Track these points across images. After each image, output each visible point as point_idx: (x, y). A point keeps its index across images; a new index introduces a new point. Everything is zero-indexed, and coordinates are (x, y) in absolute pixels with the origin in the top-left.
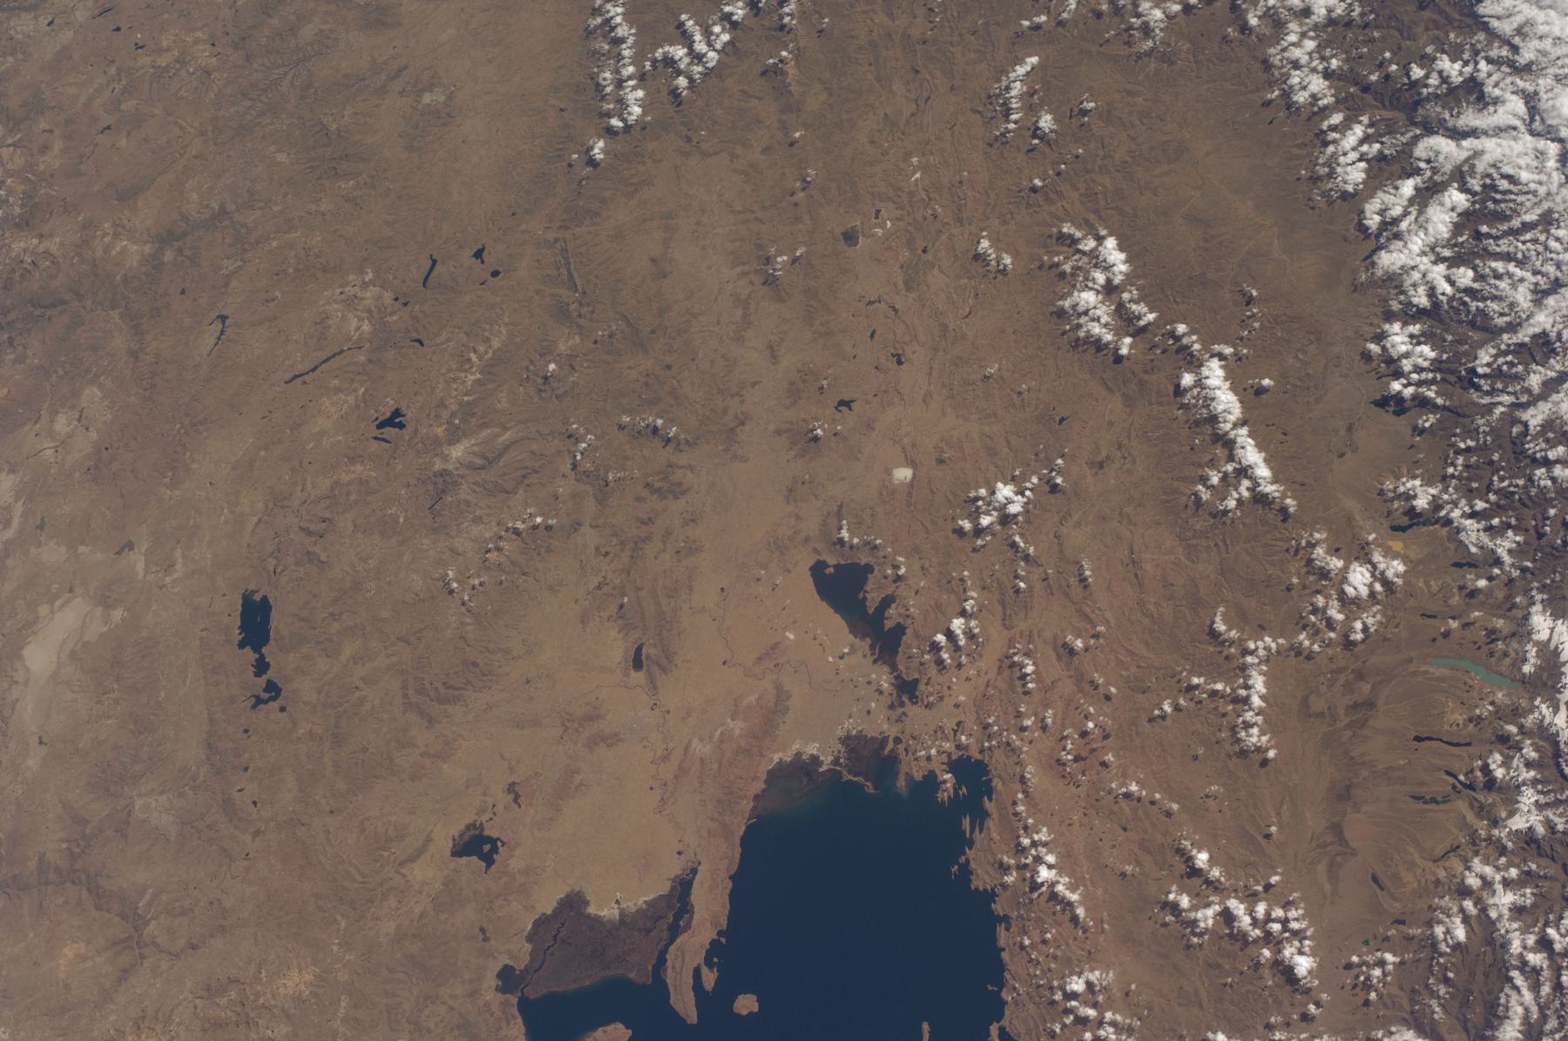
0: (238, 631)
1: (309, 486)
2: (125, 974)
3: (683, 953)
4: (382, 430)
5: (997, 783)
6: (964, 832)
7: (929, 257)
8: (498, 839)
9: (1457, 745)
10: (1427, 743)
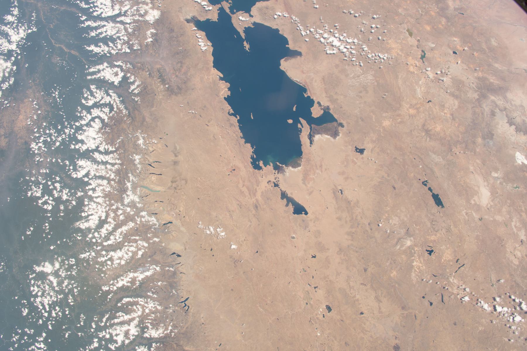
1: (442, 234)
2: (424, 125)
4: (431, 249)
6: (255, 154)
7: (305, 302)
10: (159, 174)
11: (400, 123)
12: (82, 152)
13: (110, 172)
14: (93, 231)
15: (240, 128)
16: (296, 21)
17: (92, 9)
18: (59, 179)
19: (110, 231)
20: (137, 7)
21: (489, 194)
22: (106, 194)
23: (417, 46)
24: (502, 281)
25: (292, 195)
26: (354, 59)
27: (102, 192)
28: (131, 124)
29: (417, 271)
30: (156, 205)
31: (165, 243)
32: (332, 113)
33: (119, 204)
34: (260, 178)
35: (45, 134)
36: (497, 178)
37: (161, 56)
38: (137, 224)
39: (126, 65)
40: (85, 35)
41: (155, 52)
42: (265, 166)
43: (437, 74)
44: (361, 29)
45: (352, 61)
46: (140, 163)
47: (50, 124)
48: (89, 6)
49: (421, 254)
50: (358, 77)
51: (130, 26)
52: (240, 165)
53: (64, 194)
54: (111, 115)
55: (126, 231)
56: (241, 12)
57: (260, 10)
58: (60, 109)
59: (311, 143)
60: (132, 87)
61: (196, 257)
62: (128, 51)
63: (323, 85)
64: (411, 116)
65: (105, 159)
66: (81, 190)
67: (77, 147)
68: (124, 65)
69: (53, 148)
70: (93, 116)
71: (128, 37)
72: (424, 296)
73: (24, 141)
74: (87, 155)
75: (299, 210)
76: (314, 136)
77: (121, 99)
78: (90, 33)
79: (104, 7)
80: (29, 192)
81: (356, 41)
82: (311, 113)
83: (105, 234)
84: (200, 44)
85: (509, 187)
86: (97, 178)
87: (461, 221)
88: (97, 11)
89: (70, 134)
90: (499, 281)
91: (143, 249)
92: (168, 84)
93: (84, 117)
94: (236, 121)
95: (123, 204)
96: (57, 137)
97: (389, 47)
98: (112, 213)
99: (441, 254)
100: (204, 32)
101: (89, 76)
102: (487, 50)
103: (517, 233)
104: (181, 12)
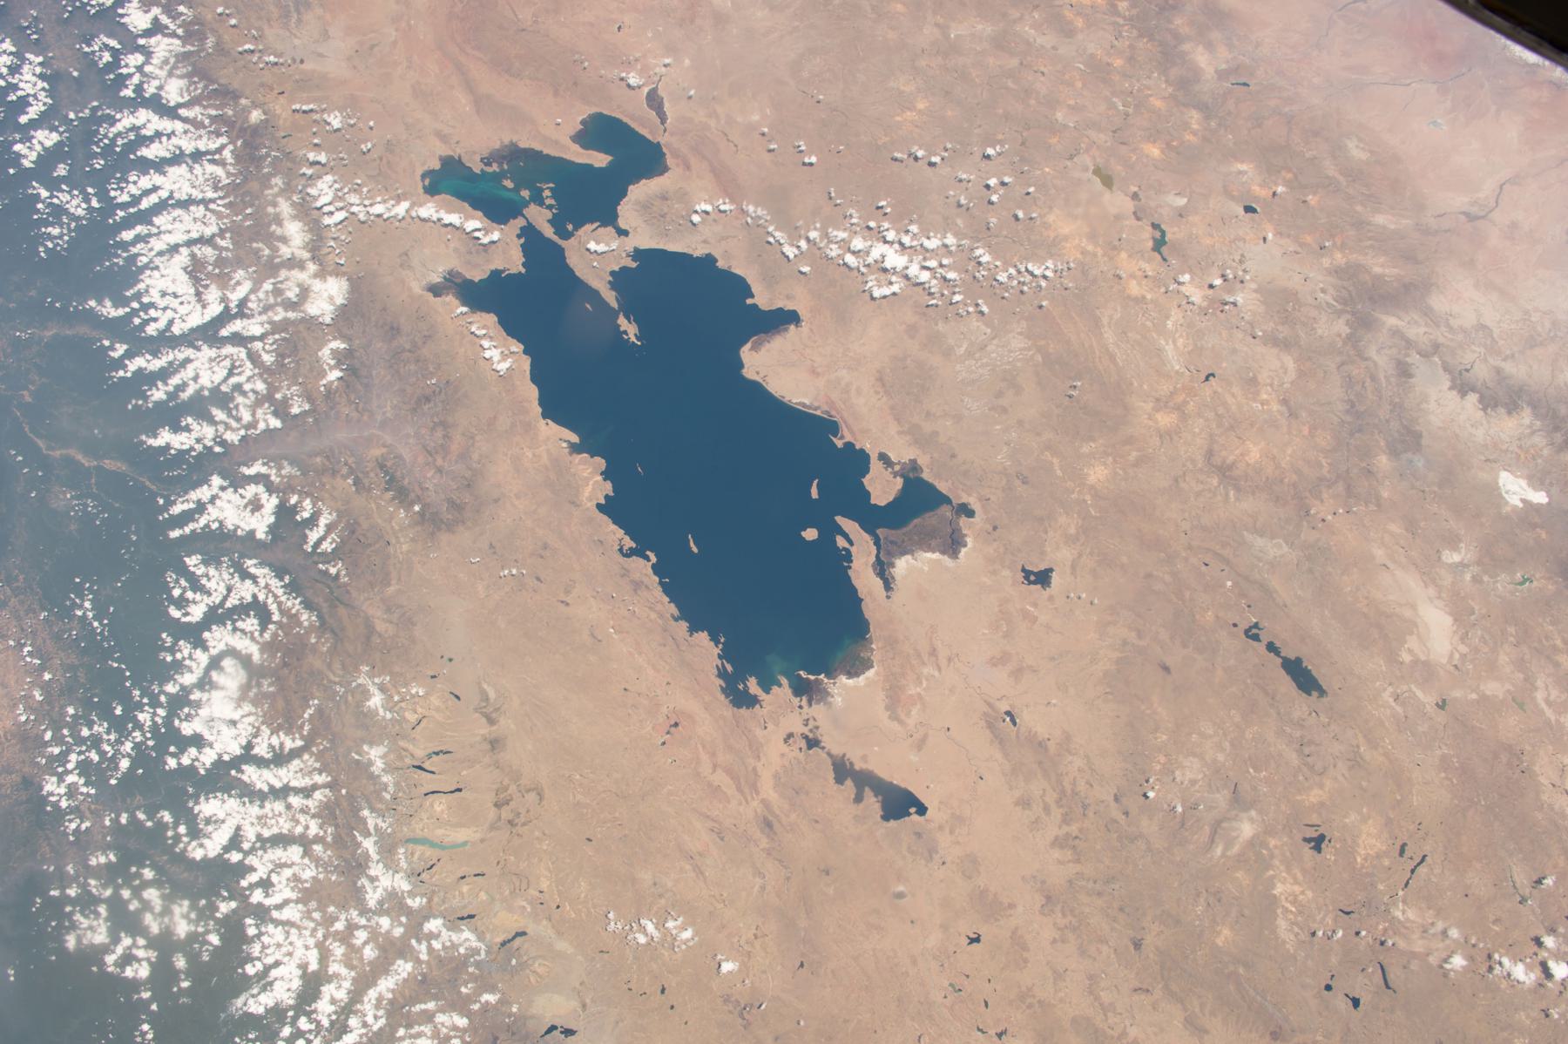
0: (1309, 668)
1: (1341, 778)
2: (1210, 454)
4: (1318, 833)
5: (722, 697)
9: (433, 792)
11: (1137, 464)
12: (202, 772)
13: (302, 818)
14: (291, 1013)
15: (666, 589)
16: (759, 218)
17: (139, 317)
18: (153, 873)
19: (343, 1004)
20: (272, 280)
21: (1448, 620)
22: (306, 889)
23: (1135, 213)
24: (1549, 881)
25: (866, 762)
26: (957, 298)
27: (292, 884)
28: (333, 651)
29: (1291, 911)
30: (465, 889)
31: (519, 1003)
32: (930, 481)
33: (354, 913)
34: (759, 732)
35: (81, 741)
36: (1463, 565)
37: (379, 418)
38: (418, 961)
39: (280, 468)
40: (134, 402)
41: (357, 410)
42: (767, 691)
43: (1211, 286)
44: (957, 199)
45: (951, 304)
46: (389, 769)
47: (87, 705)
48: (128, 310)
49: (1292, 853)
50: (982, 349)
51: (265, 344)
53: (177, 918)
54: (267, 636)
55: (393, 991)
56: (589, 227)
57: (645, 207)
58: (107, 654)
59: (888, 586)
60: (313, 536)
61: (621, 1024)
62: (275, 423)
63: (885, 399)
64: (1167, 435)
65: (281, 779)
66: (226, 894)
67: (186, 761)
68: (274, 471)
69: (113, 782)
70: (213, 652)
71: (265, 381)
72: (1330, 983)
73: (19, 779)
74: (222, 778)
75: (900, 804)
76: (892, 565)
77: (287, 579)
78: (149, 393)
79: (175, 303)
80: (68, 938)
81: (950, 240)
82: (868, 494)
83: (329, 1015)
84: (487, 354)
85: (1502, 584)
86: (268, 845)
87: (1387, 724)
88: (155, 320)
89: (155, 723)
90: (1539, 882)
91: (455, 1037)
92: (418, 500)
93: (187, 662)
94: (650, 571)
95: (364, 911)
96: (119, 742)
97: (1052, 235)
98: (337, 944)
99: (1349, 841)
100: (492, 315)
101: (173, 529)
102: (1341, 178)
103: (1557, 721)
104: (410, 267)
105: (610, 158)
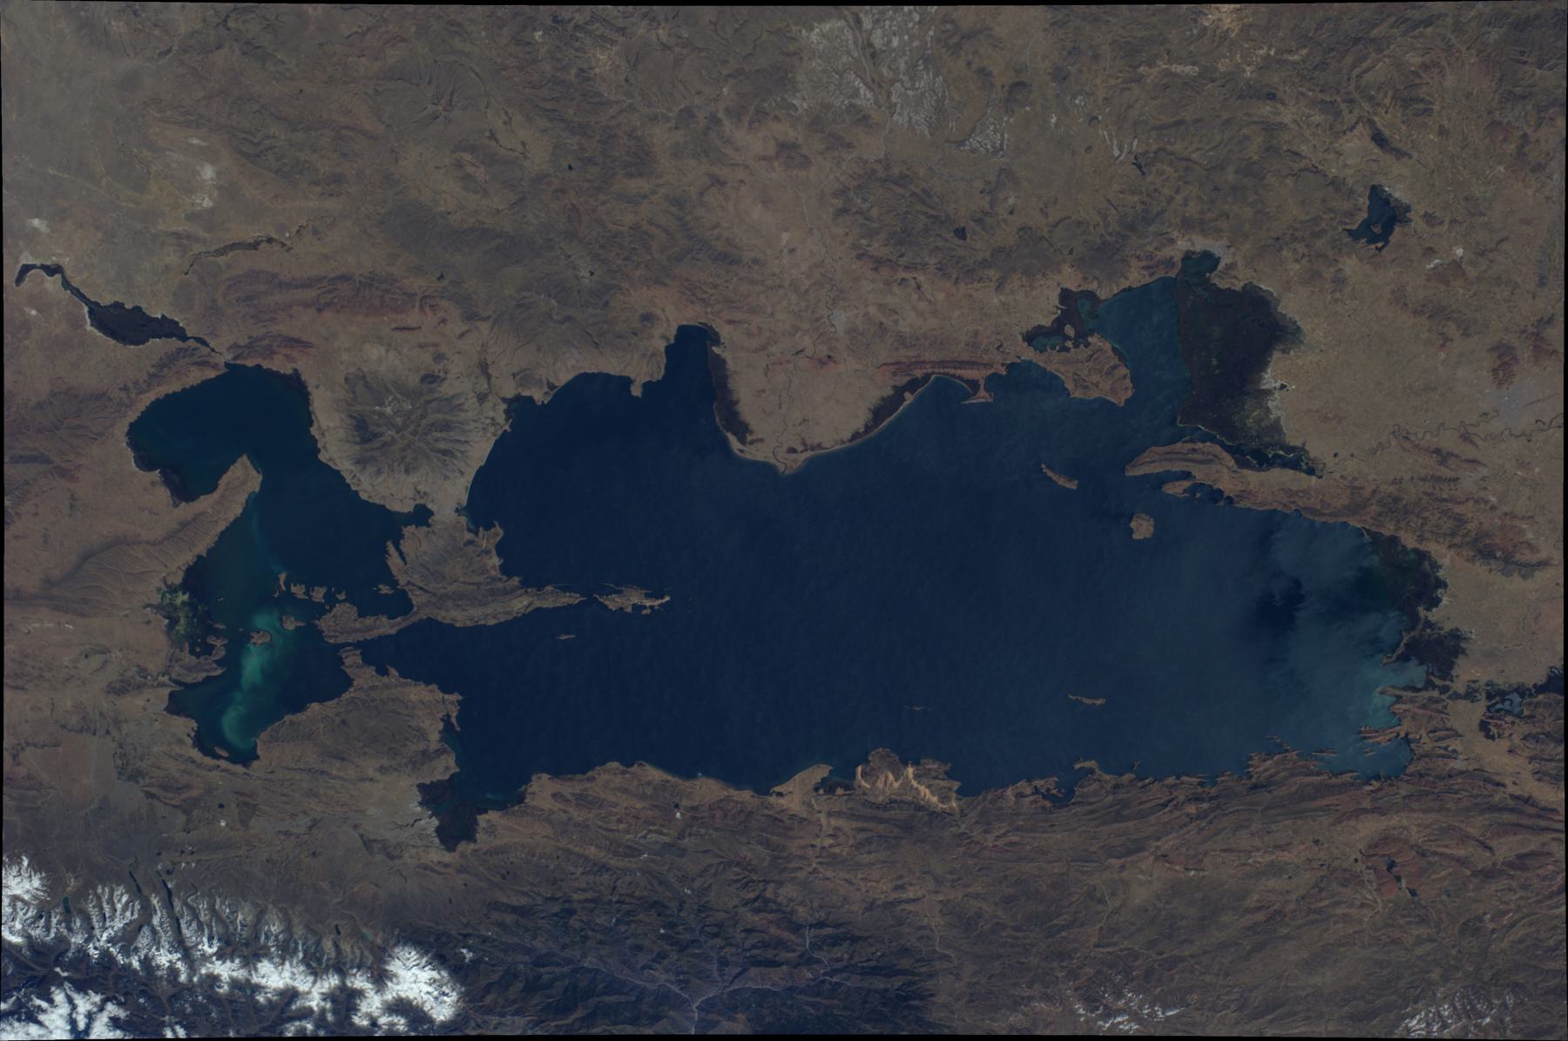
3: (1211, 461)
8: (1387, 242)
52: (1369, 828)
56: (394, 561)
105: (244, 459)
